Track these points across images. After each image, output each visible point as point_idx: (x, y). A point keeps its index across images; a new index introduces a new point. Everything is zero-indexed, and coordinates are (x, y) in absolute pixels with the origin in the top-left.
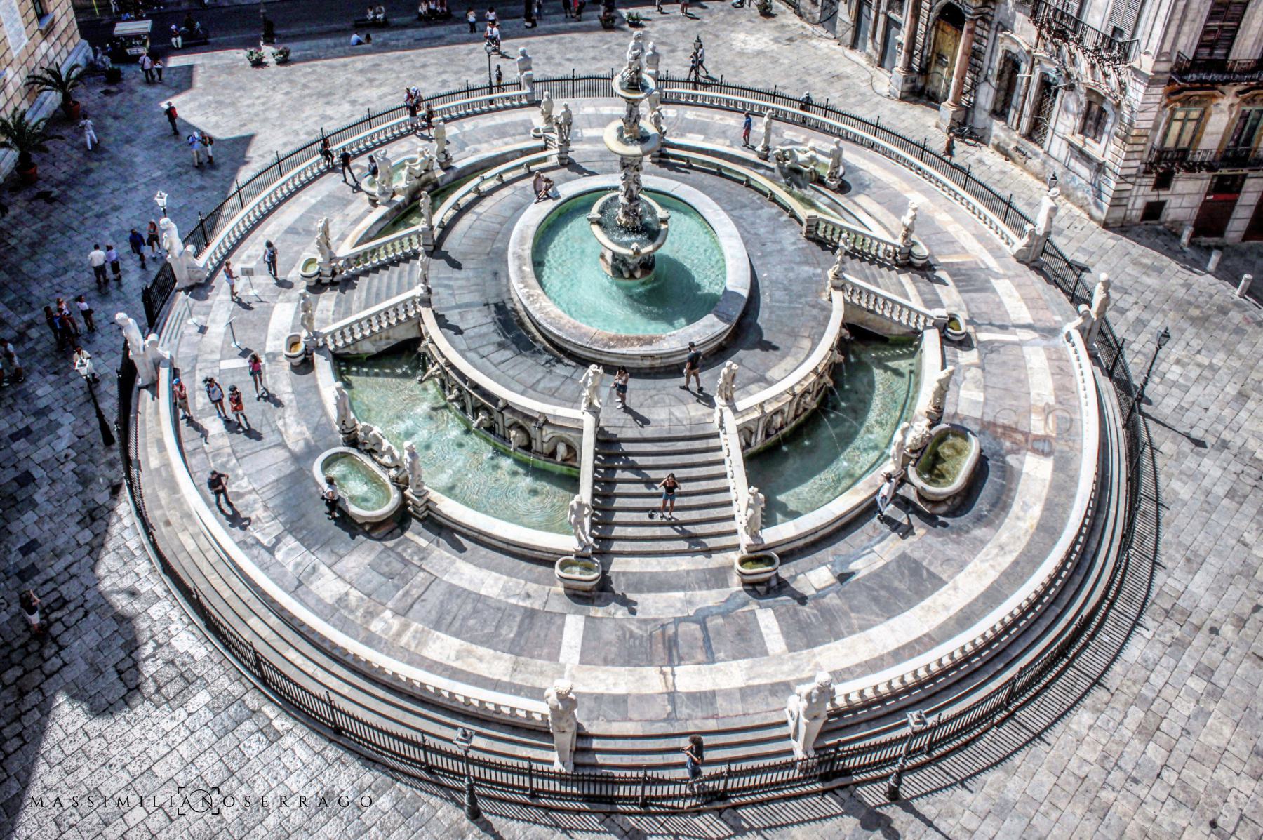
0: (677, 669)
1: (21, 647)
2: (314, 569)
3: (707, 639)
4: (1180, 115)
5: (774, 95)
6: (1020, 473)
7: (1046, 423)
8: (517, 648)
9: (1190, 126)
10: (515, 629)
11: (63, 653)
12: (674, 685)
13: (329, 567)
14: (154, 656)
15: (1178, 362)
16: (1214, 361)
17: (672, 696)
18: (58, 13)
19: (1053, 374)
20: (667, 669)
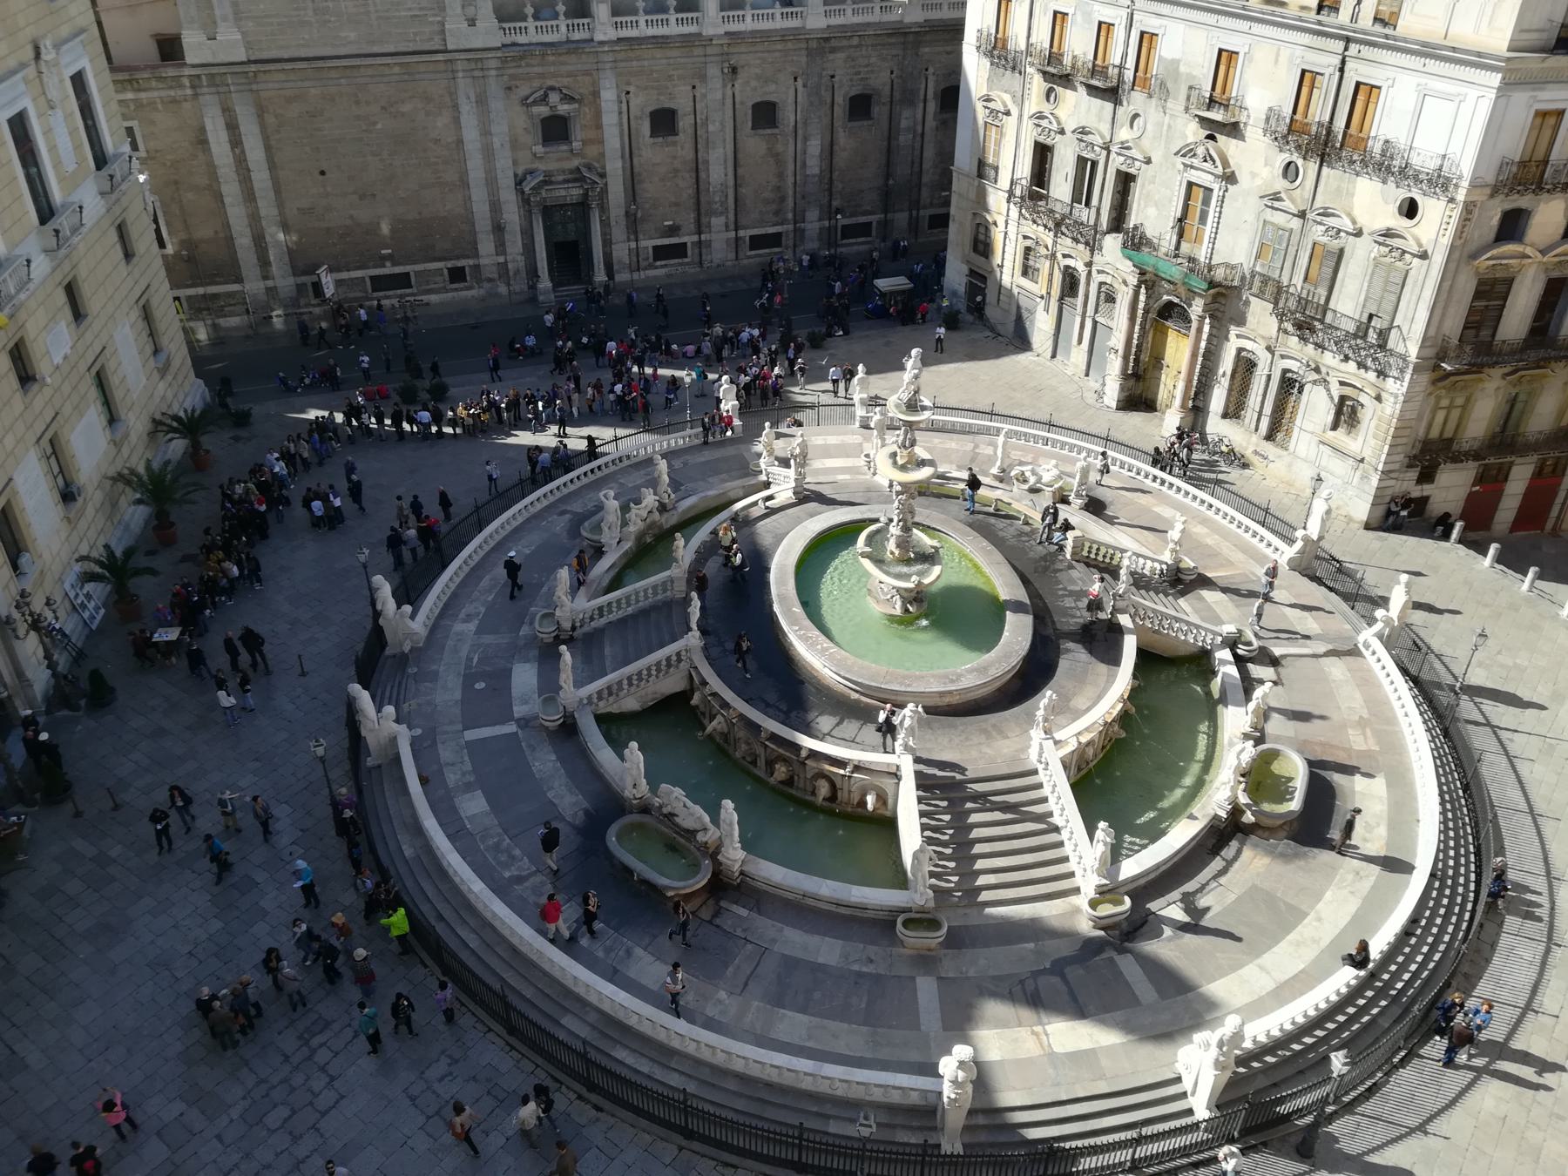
0: (1049, 1028)
1: (281, 1082)
2: (629, 953)
3: (1071, 993)
4: (1445, 402)
5: (992, 414)
6: (1353, 792)
7: (1366, 738)
8: (870, 1018)
9: (1455, 414)
10: (865, 999)
11: (336, 1084)
12: (1050, 1045)
13: (645, 950)
14: (451, 1074)
15: (1480, 665)
16: (1518, 661)
17: (1052, 1056)
18: (173, 347)
19: (1358, 685)
20: (1038, 1029)
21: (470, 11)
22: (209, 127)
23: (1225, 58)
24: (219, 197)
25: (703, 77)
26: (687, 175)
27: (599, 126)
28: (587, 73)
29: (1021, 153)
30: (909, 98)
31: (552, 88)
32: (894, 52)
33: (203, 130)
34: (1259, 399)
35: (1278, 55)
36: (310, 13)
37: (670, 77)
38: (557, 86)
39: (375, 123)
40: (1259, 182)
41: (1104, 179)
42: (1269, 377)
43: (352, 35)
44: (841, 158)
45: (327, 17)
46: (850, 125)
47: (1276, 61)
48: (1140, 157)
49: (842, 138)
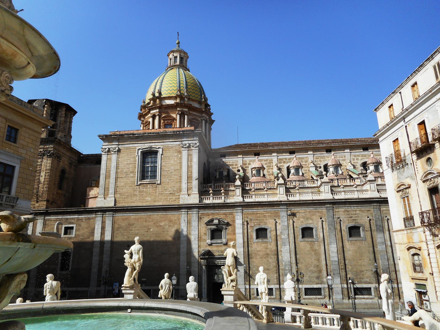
21: (189, 192)
22: (96, 227)
24: (92, 252)
25: (279, 217)
26: (273, 257)
27: (234, 234)
28: (231, 214)
31: (216, 219)
32: (367, 209)
33: (94, 228)
36: (138, 192)
37: (265, 216)
38: (219, 218)
39: (150, 229)
43: (149, 199)
44: (348, 254)
45: (143, 193)
46: (351, 239)
49: (347, 245)
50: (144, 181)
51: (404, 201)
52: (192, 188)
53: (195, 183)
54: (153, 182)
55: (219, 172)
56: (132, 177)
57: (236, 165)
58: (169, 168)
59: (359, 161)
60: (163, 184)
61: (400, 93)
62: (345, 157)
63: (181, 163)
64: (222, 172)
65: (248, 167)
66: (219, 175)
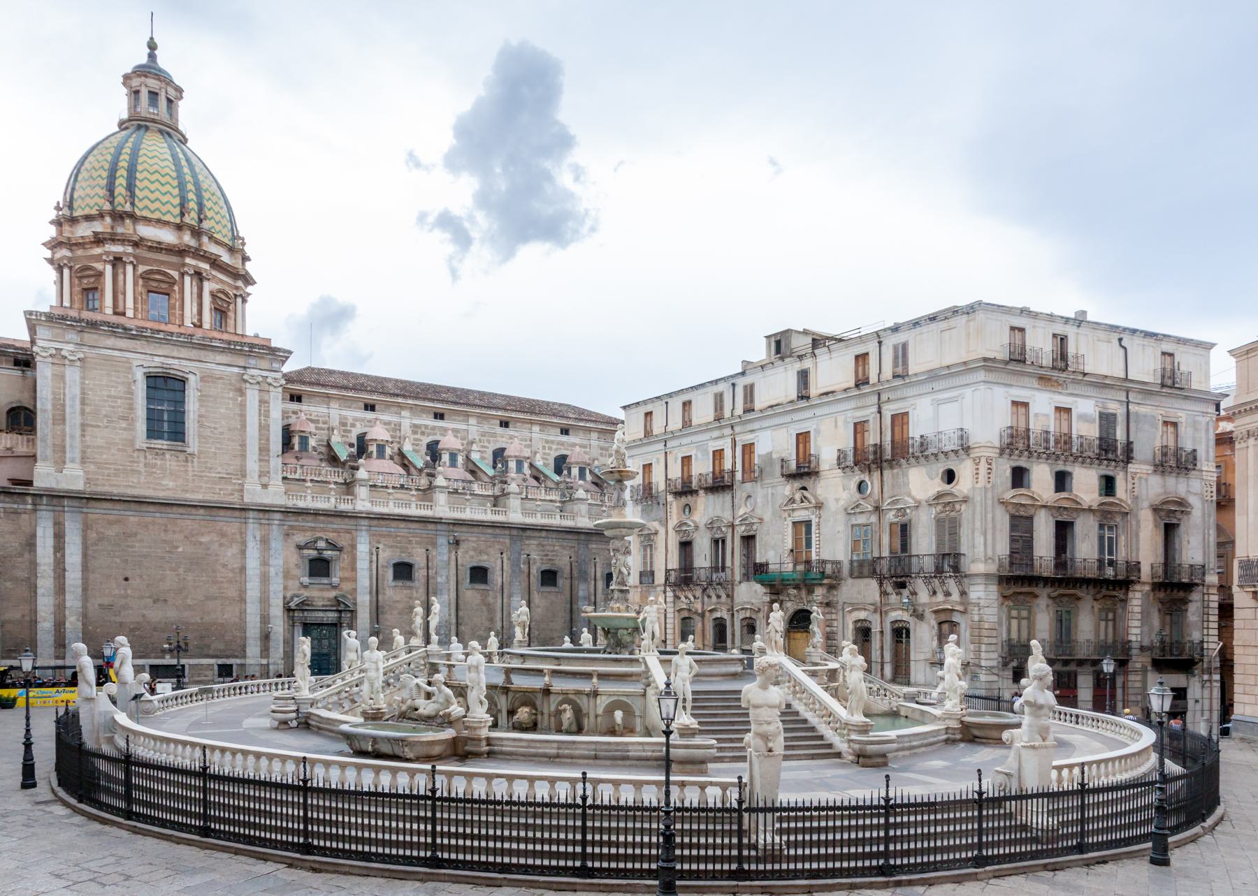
23: (803, 439)
29: (669, 556)
30: (584, 576)
34: (879, 652)
35: (836, 422)
40: (842, 503)
41: (733, 549)
42: (882, 632)
47: (836, 426)
48: (755, 520)
50: (156, 441)
51: (645, 550)
52: (269, 472)
53: (276, 463)
54: (180, 448)
55: (301, 437)
56: (125, 429)
57: (325, 423)
58: (216, 423)
59: (552, 452)
60: (202, 456)
61: (667, 403)
62: (531, 440)
63: (243, 416)
64: (306, 438)
65: (350, 431)
66: (301, 443)
